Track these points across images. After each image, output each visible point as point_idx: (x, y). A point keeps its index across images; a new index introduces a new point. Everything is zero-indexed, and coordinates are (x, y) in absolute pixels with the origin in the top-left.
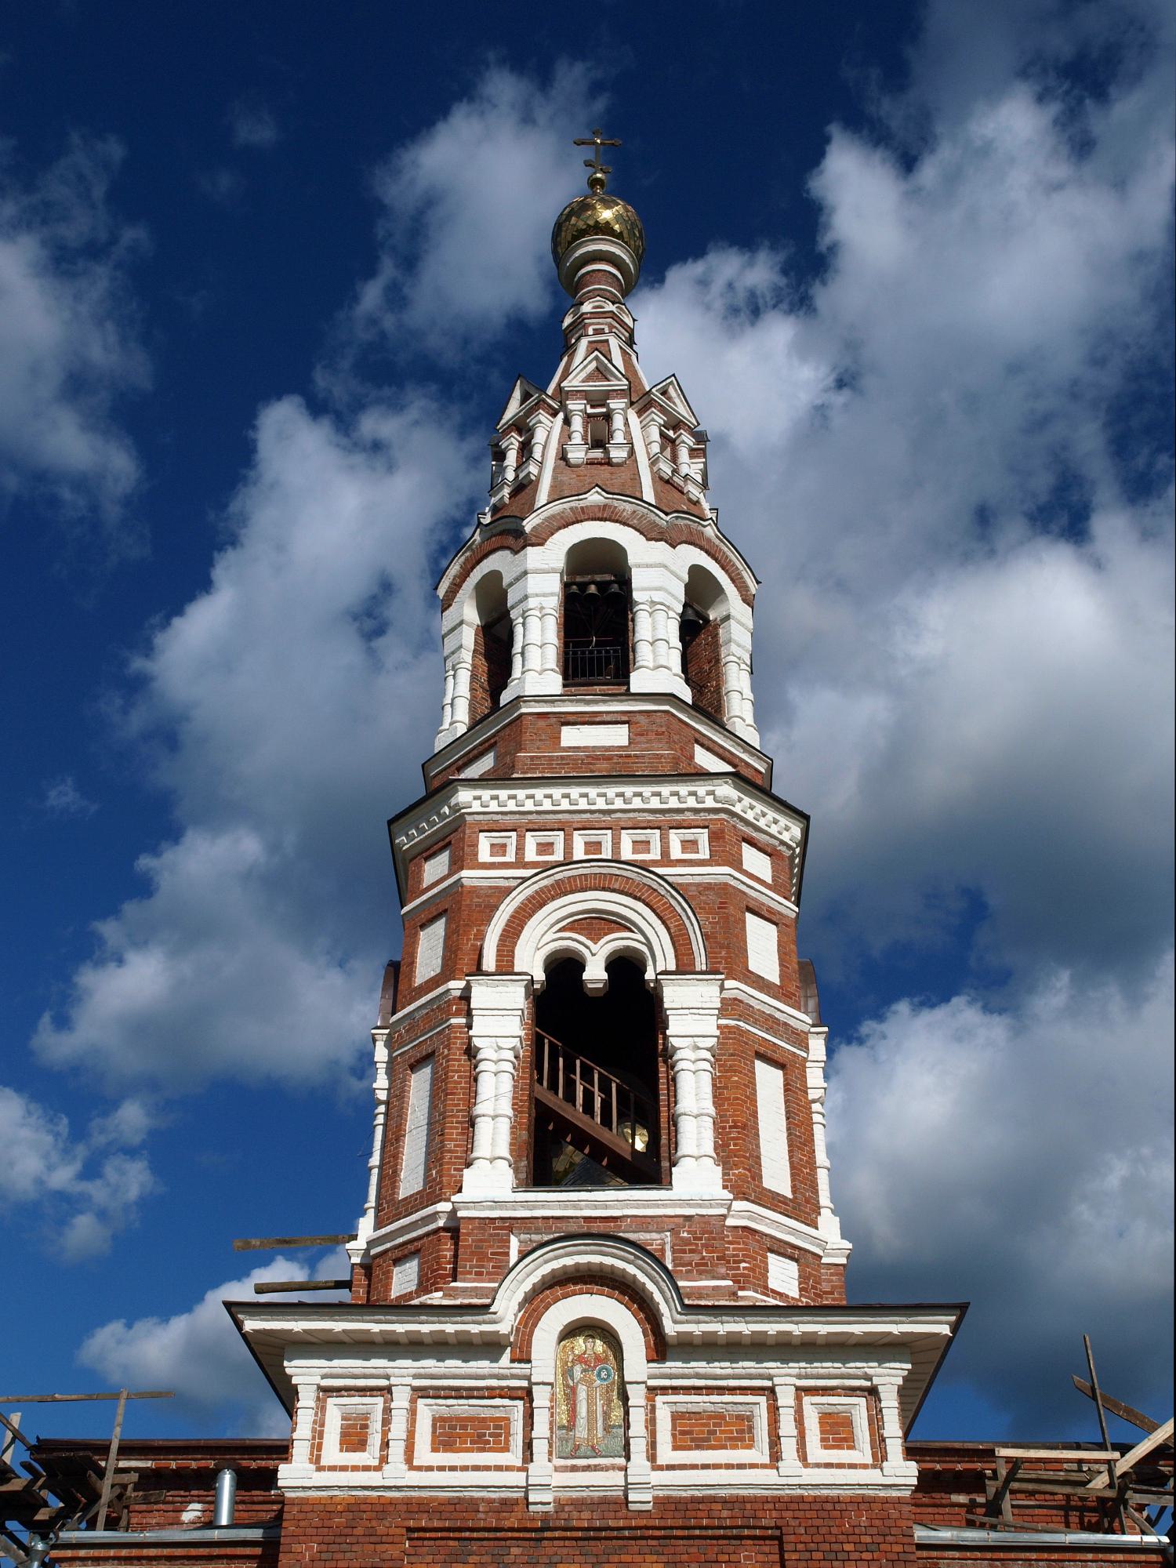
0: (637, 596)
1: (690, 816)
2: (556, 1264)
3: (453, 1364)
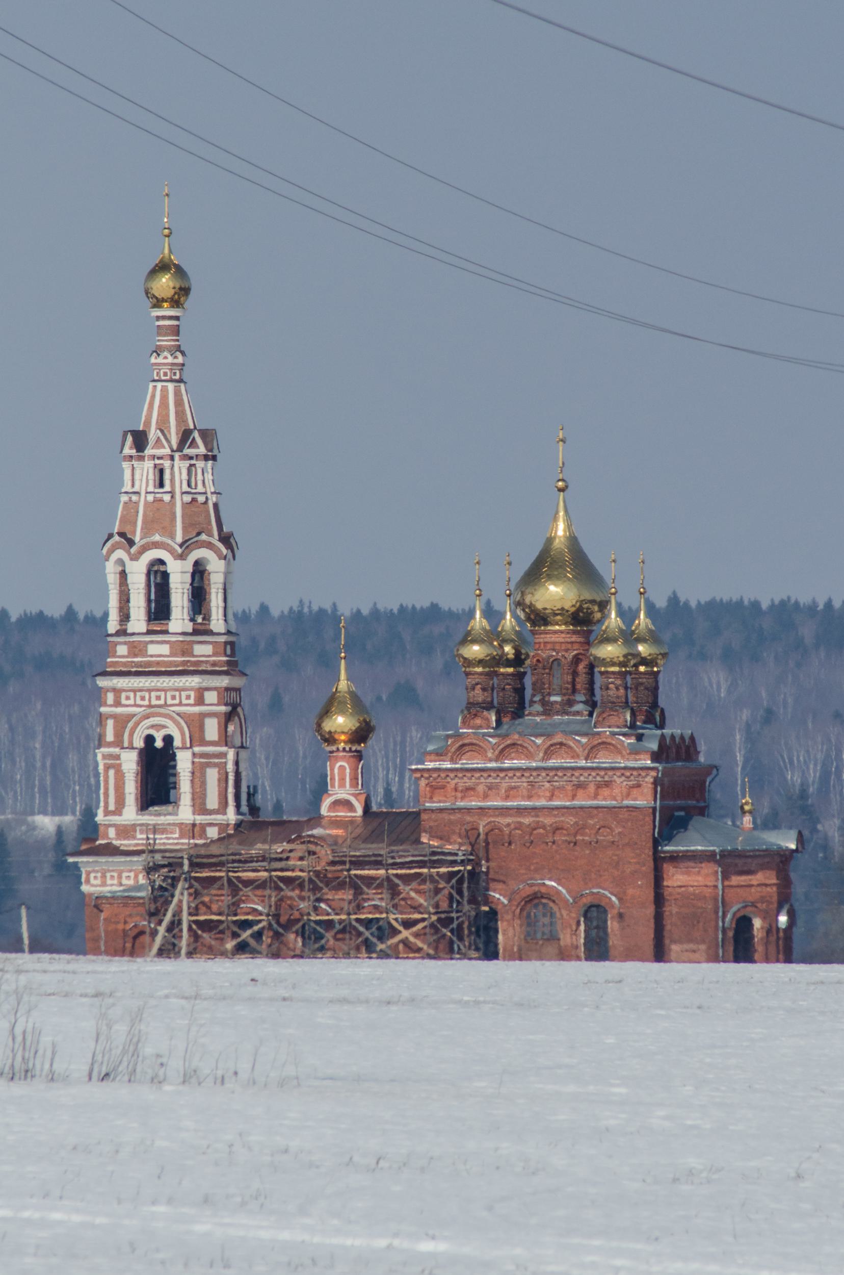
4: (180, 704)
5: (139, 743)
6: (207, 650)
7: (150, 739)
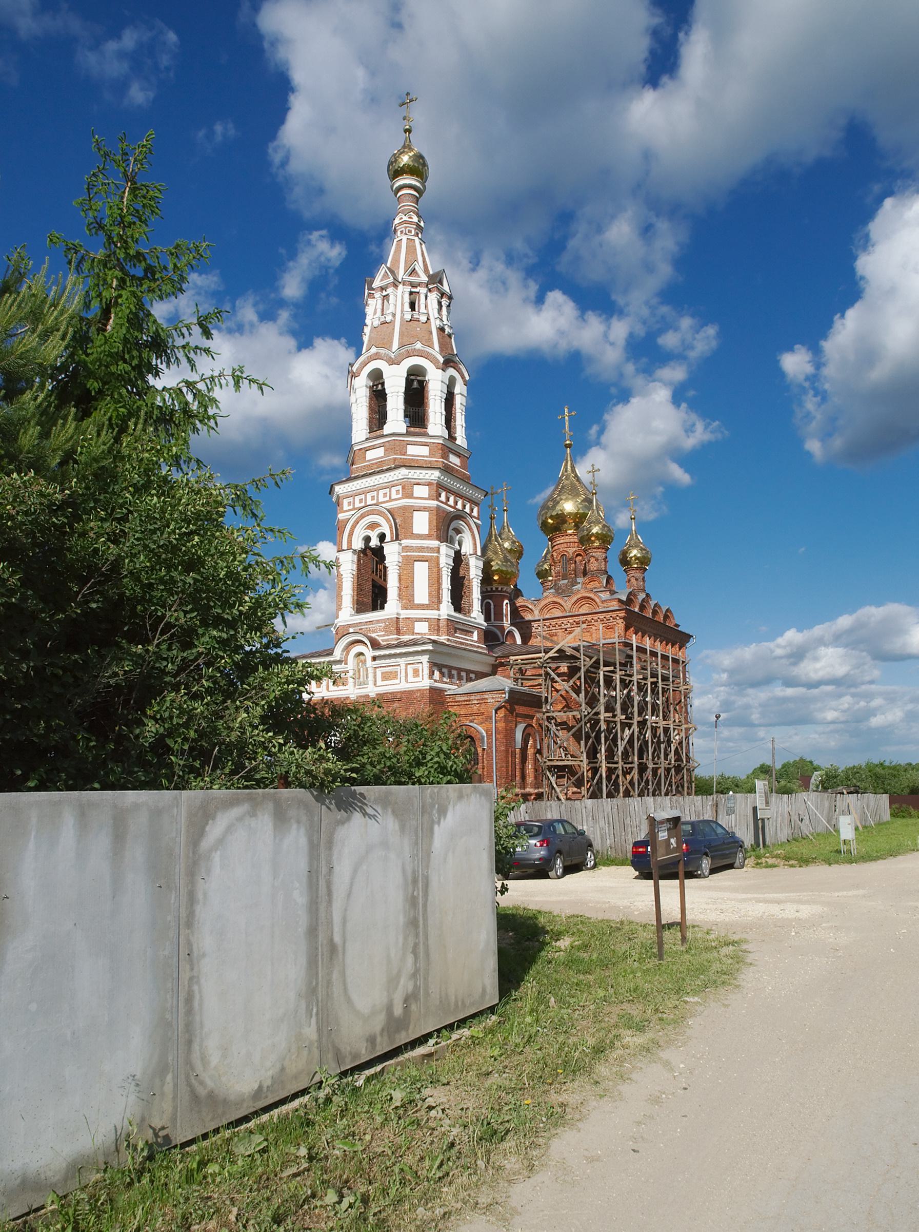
0: (387, 391)
1: (396, 482)
2: (348, 640)
4: (391, 500)
5: (358, 544)
6: (424, 451)
7: (367, 539)
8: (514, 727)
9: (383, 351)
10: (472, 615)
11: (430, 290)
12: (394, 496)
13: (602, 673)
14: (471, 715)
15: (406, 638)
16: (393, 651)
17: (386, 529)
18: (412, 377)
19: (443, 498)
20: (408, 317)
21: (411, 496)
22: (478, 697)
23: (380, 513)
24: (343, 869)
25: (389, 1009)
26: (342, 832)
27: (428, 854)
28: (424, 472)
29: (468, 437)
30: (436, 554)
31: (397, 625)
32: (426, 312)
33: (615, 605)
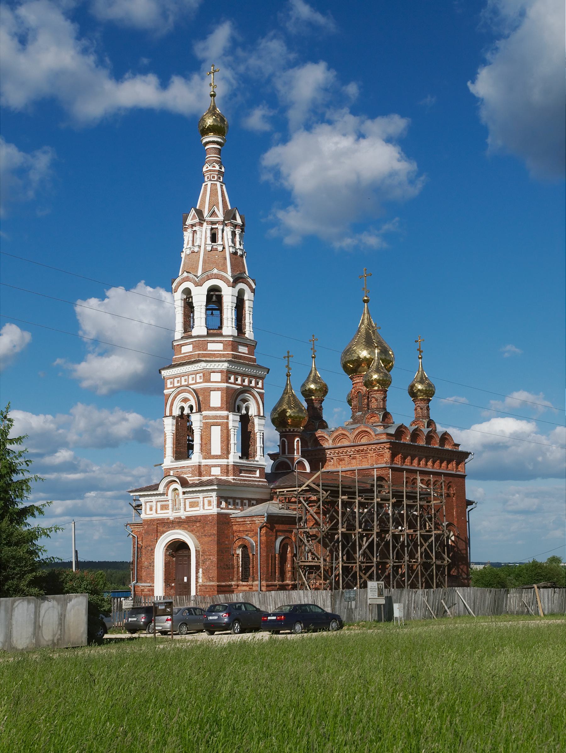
2: (168, 480)
3: (159, 497)
4: (196, 383)
5: (176, 412)
6: (220, 346)
7: (182, 409)
8: (274, 539)
9: (191, 276)
10: (256, 459)
11: (226, 225)
12: (198, 380)
13: (340, 500)
14: (246, 531)
15: (205, 478)
16: (194, 489)
17: (193, 402)
18: (212, 293)
19: (232, 380)
20: (209, 248)
21: (208, 381)
22: (250, 519)
23: (189, 392)
24: (42, 612)
25: (53, 640)
26: (42, 605)
27: (65, 610)
28: (217, 364)
29: (255, 328)
30: (226, 421)
31: (199, 470)
32: (221, 243)
33: (384, 439)
